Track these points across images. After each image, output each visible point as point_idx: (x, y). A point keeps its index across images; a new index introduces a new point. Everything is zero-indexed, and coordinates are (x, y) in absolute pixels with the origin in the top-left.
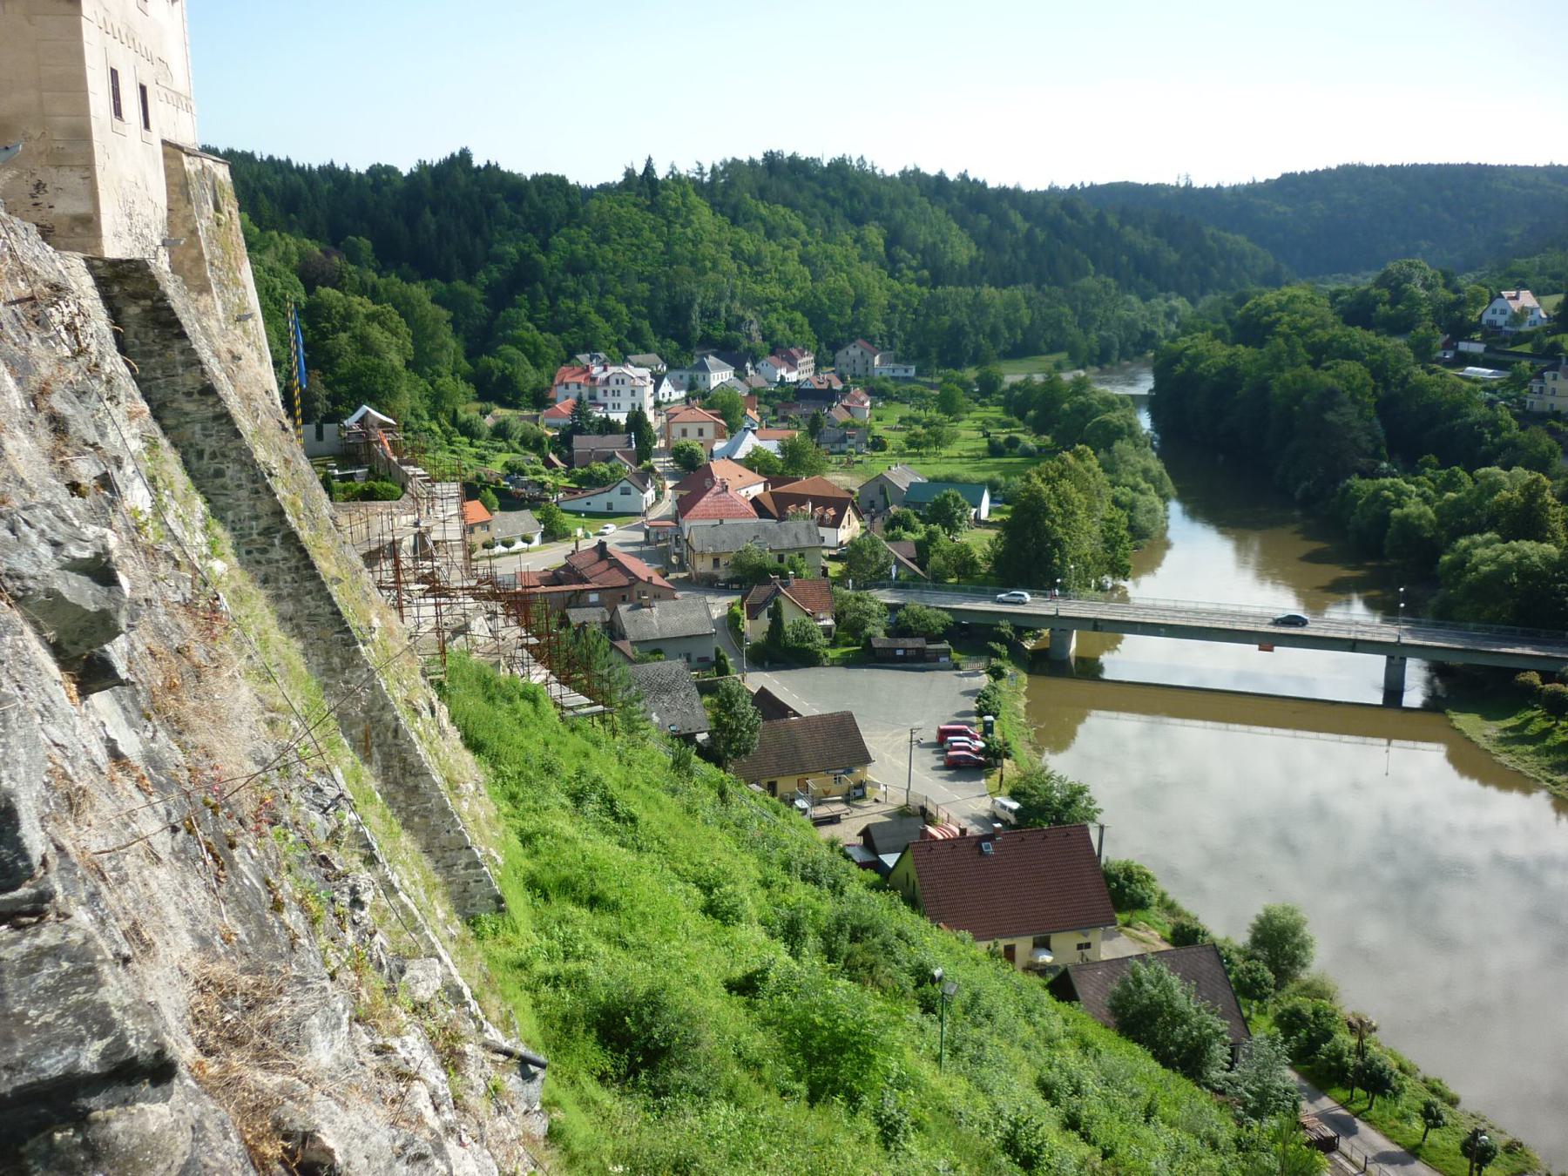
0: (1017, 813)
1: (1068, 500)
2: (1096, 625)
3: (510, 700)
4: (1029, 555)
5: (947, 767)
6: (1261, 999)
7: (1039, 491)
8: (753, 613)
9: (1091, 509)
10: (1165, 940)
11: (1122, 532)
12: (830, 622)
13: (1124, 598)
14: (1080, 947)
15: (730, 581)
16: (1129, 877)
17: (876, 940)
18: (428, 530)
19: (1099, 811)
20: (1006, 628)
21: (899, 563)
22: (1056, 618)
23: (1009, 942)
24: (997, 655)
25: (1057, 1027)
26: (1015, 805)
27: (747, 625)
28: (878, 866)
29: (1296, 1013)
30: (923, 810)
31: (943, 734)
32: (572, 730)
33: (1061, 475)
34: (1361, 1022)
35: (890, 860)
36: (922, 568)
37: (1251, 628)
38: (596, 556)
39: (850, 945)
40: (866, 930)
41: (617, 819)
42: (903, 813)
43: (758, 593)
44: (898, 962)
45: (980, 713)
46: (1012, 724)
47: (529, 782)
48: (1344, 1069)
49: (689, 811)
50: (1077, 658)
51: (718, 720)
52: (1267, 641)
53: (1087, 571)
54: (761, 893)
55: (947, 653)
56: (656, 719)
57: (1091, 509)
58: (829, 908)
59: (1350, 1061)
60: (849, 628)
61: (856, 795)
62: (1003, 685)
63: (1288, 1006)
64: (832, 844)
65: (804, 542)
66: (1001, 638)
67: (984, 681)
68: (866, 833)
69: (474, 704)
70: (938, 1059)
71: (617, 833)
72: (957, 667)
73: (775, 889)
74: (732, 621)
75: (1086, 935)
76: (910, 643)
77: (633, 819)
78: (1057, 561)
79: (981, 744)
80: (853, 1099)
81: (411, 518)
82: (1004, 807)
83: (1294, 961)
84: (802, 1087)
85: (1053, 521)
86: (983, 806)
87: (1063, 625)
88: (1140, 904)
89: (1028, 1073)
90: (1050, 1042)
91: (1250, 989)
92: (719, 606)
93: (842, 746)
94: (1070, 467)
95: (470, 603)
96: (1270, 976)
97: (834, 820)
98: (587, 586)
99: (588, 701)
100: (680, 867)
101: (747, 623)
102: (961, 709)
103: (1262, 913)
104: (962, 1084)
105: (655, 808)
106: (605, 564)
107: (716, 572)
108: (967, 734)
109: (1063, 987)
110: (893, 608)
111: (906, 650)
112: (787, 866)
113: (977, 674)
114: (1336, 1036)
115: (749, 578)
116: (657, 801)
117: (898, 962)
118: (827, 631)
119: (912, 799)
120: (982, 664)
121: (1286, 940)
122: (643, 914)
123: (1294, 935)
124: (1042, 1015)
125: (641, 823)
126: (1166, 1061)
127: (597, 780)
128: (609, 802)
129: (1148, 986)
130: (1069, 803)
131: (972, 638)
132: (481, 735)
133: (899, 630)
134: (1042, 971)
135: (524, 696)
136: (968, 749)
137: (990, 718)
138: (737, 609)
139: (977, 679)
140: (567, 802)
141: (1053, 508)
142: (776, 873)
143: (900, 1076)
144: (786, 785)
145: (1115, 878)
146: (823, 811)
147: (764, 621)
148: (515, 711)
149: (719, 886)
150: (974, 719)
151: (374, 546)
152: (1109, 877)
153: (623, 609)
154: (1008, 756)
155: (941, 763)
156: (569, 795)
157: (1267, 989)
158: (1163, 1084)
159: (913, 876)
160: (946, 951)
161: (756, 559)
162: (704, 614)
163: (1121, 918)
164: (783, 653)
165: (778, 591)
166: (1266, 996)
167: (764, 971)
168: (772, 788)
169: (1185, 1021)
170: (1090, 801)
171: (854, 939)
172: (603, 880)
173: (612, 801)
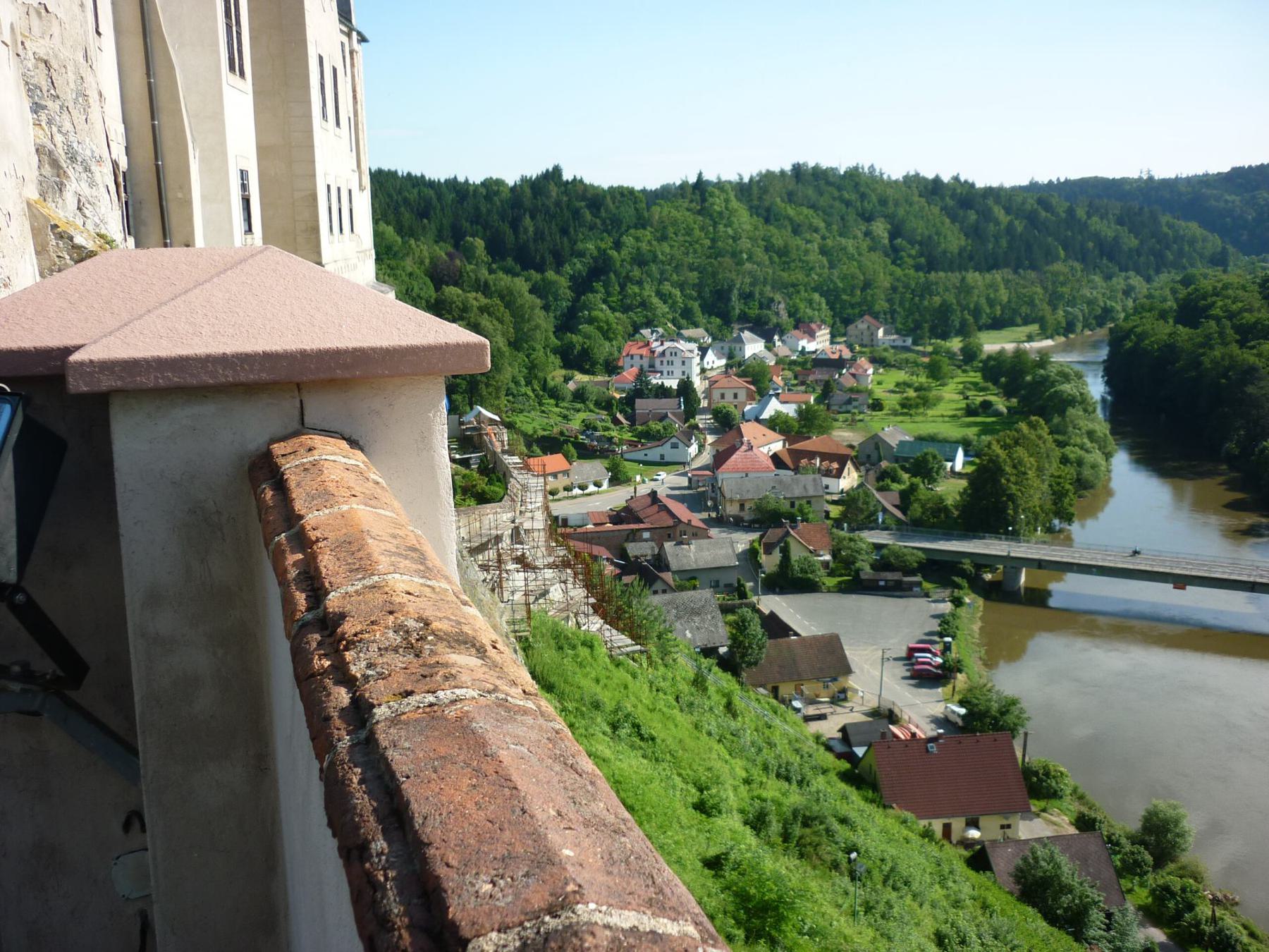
0: (963, 717)
1: (1021, 462)
2: (1040, 564)
3: (574, 647)
4: (987, 507)
5: (911, 678)
6: (1141, 876)
7: (998, 456)
8: (769, 549)
9: (1040, 470)
10: (1071, 823)
11: (1068, 487)
12: (828, 557)
13: (1068, 541)
14: (1002, 827)
15: (753, 522)
16: (1047, 774)
17: (822, 827)
18: (521, 524)
19: (1028, 719)
20: (967, 565)
21: (885, 510)
22: (1006, 559)
23: (946, 821)
24: (959, 587)
25: (966, 890)
26: (963, 711)
27: (763, 558)
28: (850, 757)
29: (1166, 888)
30: (891, 712)
31: (912, 651)
32: (618, 665)
33: (1017, 443)
34: (1225, 896)
35: (860, 751)
36: (904, 513)
37: (1168, 570)
38: (649, 500)
39: (801, 833)
40: (815, 818)
41: (642, 738)
42: (875, 713)
43: (773, 534)
44: (837, 843)
45: (941, 635)
46: (967, 648)
47: (583, 715)
48: (1202, 933)
49: (696, 727)
50: (1026, 589)
51: (733, 638)
52: (1181, 581)
53: (1036, 520)
54: (743, 789)
55: (919, 584)
56: (689, 635)
57: (1040, 470)
58: (795, 798)
59: (1209, 929)
60: (843, 563)
61: (840, 698)
62: (962, 612)
63: (1161, 882)
64: (817, 738)
65: (811, 492)
66: (963, 573)
67: (947, 607)
68: (843, 730)
69: (547, 654)
70: (854, 914)
71: (641, 748)
72: (927, 595)
73: (754, 786)
74: (751, 555)
75: (1007, 818)
76: (890, 576)
77: (653, 739)
78: (1010, 512)
79: (939, 660)
80: (773, 942)
81: (510, 515)
82: (954, 712)
83: (1174, 846)
84: (740, 933)
85: (1008, 480)
86: (938, 710)
87: (1015, 564)
88: (1054, 795)
89: (929, 926)
90: (957, 904)
91: (1131, 868)
92: (743, 541)
93: (830, 662)
94: (1024, 436)
95: (549, 573)
96: (1149, 858)
97: (822, 717)
98: (642, 526)
99: (629, 641)
100: (683, 772)
101: (764, 557)
102: (927, 630)
103: (1150, 807)
104: (870, 933)
105: (672, 727)
106: (655, 508)
107: (742, 514)
108: (929, 651)
109: (979, 860)
110: (879, 547)
111: (886, 581)
112: (766, 768)
113: (943, 601)
114: (1197, 909)
115: (768, 519)
116: (674, 720)
117: (837, 843)
118: (826, 565)
119: (882, 703)
120: (948, 592)
121: (1168, 831)
122: (649, 814)
123: (1176, 826)
124: (955, 882)
125: (659, 741)
126: (1052, 919)
127: (627, 716)
128: (636, 726)
129: (1043, 864)
130: (1004, 712)
131: (941, 571)
132: (553, 679)
133: (883, 565)
134: (966, 843)
135: (584, 644)
136: (929, 664)
137: (948, 639)
138: (756, 545)
139: (941, 606)
140: (608, 729)
141: (1008, 469)
142: (756, 773)
143: (811, 928)
144: (786, 690)
145: (1036, 773)
146: (811, 711)
147: (777, 556)
148: (577, 656)
149: (708, 788)
150: (936, 638)
151: (485, 540)
152: (1027, 772)
153: (668, 546)
154: (960, 671)
155: (908, 674)
156: (609, 724)
157: (1146, 868)
158: (1045, 941)
159: (875, 768)
160: (879, 830)
161: (772, 505)
162: (730, 551)
163: (1035, 805)
164: (790, 581)
165: (788, 532)
166: (1146, 873)
167: (726, 854)
168: (775, 692)
169: (1071, 891)
170: (1022, 711)
171: (805, 824)
172: (625, 791)
173: (638, 727)
